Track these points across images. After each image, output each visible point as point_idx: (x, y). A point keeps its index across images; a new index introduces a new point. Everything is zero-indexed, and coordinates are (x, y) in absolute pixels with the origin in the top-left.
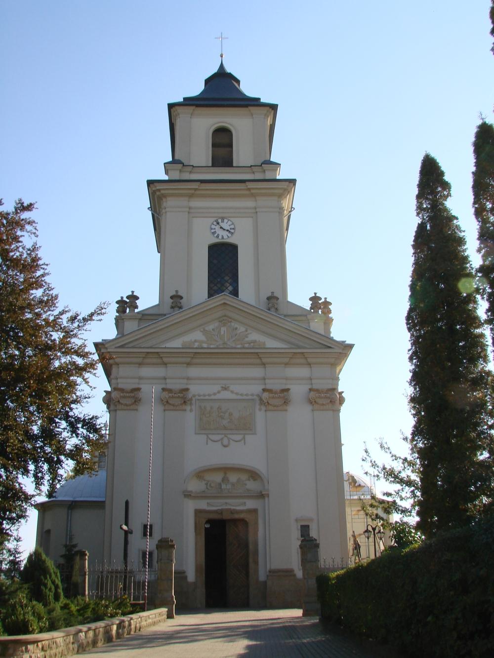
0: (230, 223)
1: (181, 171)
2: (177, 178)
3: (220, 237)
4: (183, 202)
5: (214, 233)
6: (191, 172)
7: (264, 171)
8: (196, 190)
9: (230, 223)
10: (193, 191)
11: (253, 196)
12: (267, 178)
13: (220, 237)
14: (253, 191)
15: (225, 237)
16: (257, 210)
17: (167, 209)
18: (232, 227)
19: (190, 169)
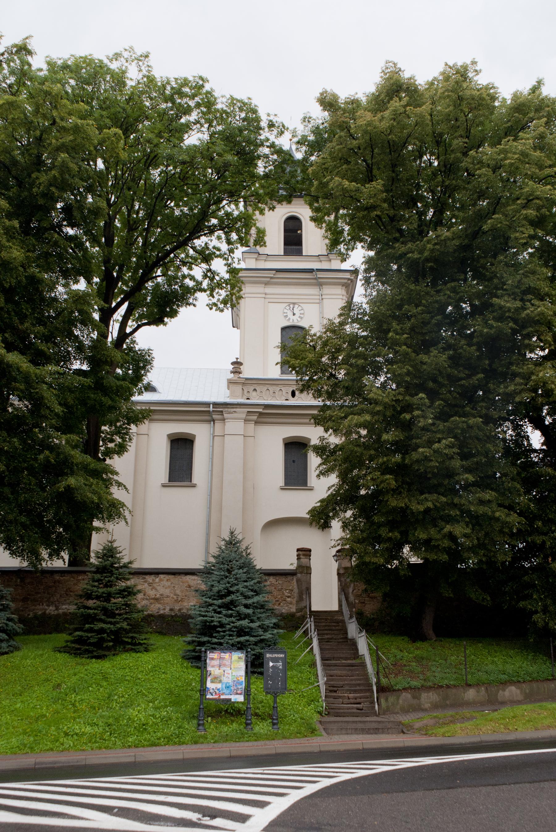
0: (300, 308)
1: (256, 259)
2: (253, 267)
3: (291, 321)
4: (260, 289)
5: (286, 316)
6: (265, 260)
7: (330, 260)
8: (271, 278)
9: (300, 308)
10: (268, 279)
11: (320, 285)
12: (333, 268)
13: (291, 321)
14: (320, 280)
15: (295, 321)
16: (323, 297)
17: (246, 295)
18: (302, 312)
19: (264, 257)
